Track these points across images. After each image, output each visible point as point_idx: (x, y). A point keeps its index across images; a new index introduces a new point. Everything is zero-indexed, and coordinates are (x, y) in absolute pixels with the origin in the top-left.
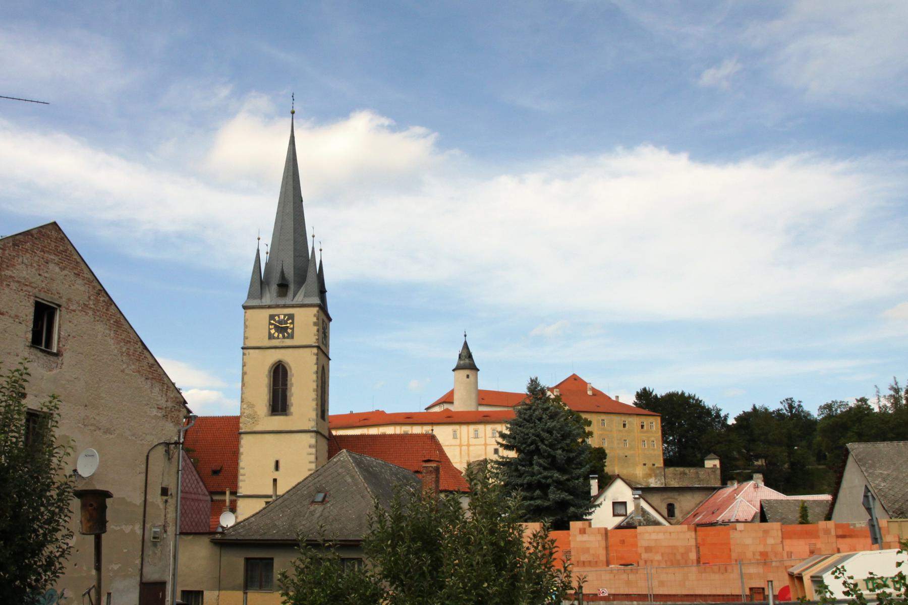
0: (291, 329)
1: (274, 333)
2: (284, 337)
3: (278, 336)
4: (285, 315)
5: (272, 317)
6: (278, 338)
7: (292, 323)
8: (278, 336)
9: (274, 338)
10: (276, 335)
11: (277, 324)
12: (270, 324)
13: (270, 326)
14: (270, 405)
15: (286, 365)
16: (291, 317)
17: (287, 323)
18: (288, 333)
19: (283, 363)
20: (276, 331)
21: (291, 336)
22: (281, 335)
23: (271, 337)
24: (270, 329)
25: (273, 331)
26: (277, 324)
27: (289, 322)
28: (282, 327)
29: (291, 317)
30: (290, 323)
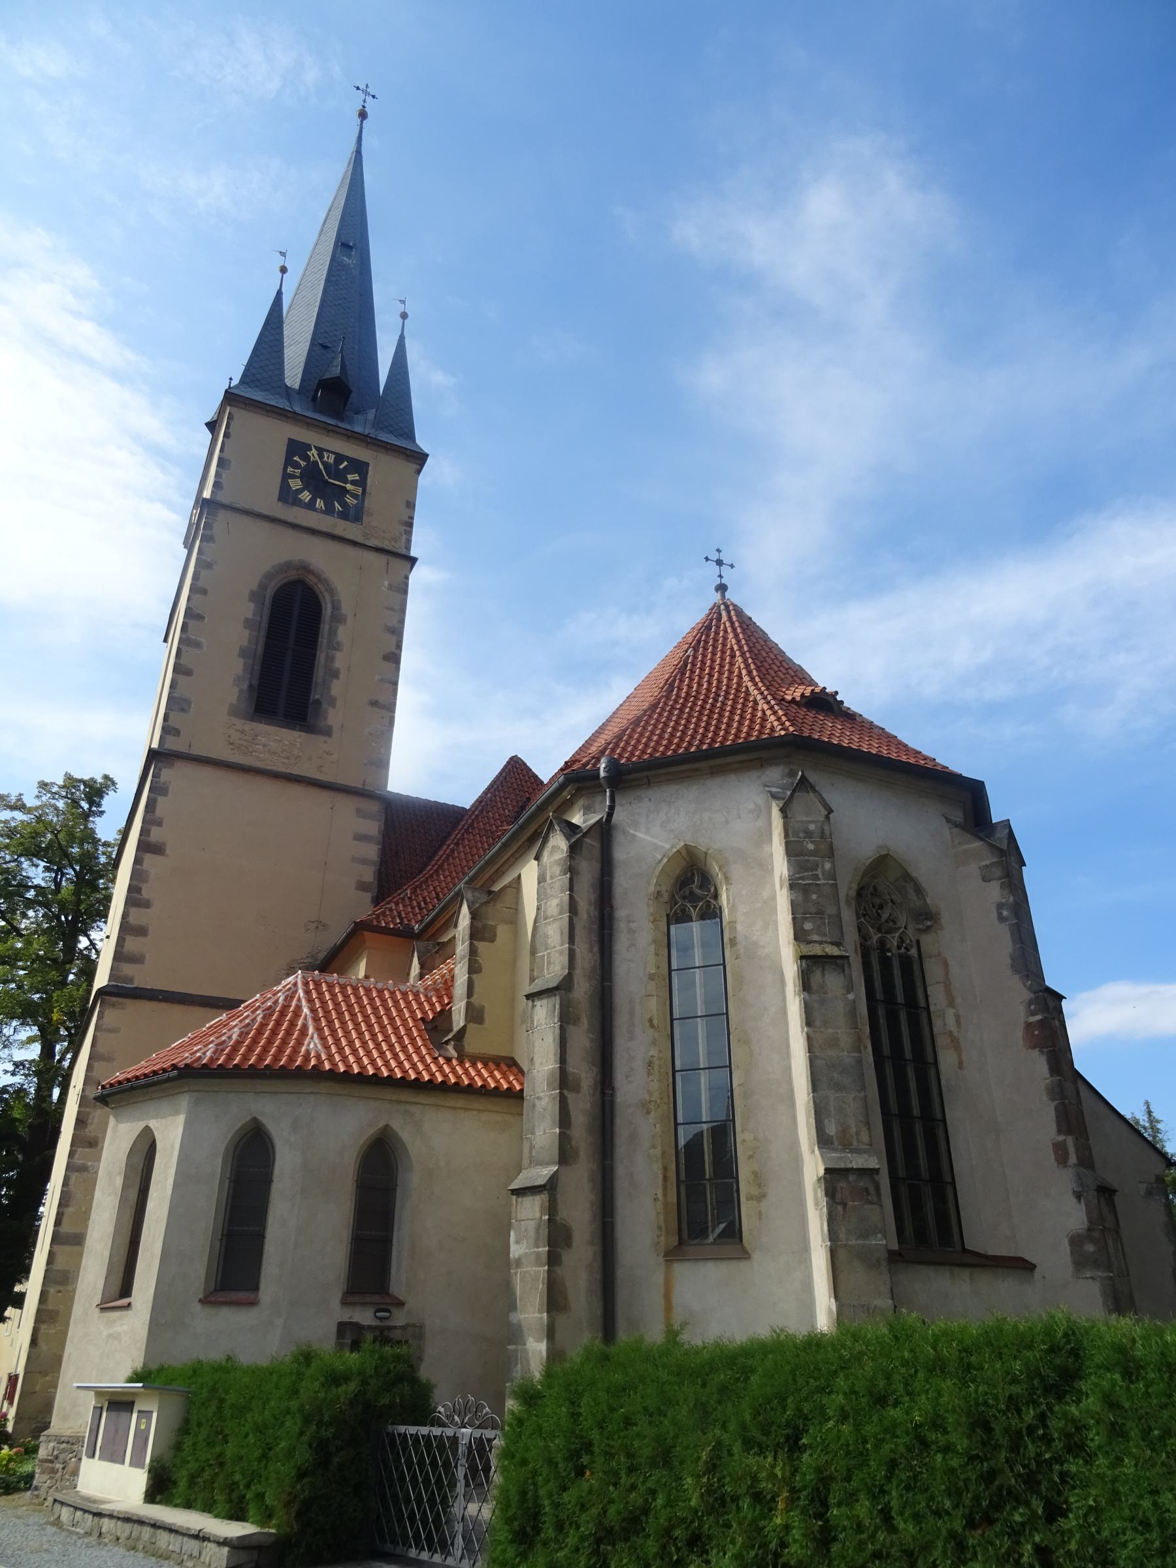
0: (355, 496)
1: (300, 491)
2: (329, 510)
3: (312, 502)
4: (340, 458)
5: (296, 448)
6: (311, 505)
7: (362, 483)
8: (312, 502)
9: (297, 502)
10: (306, 496)
11: (321, 466)
12: (289, 461)
13: (290, 470)
14: (251, 686)
15: (320, 588)
16: (360, 467)
17: (346, 481)
18: (344, 504)
19: (311, 580)
20: (306, 486)
21: (354, 515)
22: (320, 503)
23: (286, 496)
24: (286, 477)
25: (295, 484)
26: (321, 466)
27: (350, 477)
28: (328, 482)
29: (360, 467)
30: (353, 483)
